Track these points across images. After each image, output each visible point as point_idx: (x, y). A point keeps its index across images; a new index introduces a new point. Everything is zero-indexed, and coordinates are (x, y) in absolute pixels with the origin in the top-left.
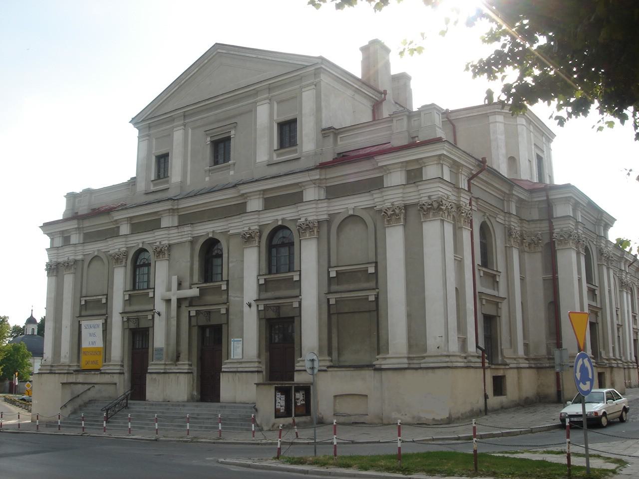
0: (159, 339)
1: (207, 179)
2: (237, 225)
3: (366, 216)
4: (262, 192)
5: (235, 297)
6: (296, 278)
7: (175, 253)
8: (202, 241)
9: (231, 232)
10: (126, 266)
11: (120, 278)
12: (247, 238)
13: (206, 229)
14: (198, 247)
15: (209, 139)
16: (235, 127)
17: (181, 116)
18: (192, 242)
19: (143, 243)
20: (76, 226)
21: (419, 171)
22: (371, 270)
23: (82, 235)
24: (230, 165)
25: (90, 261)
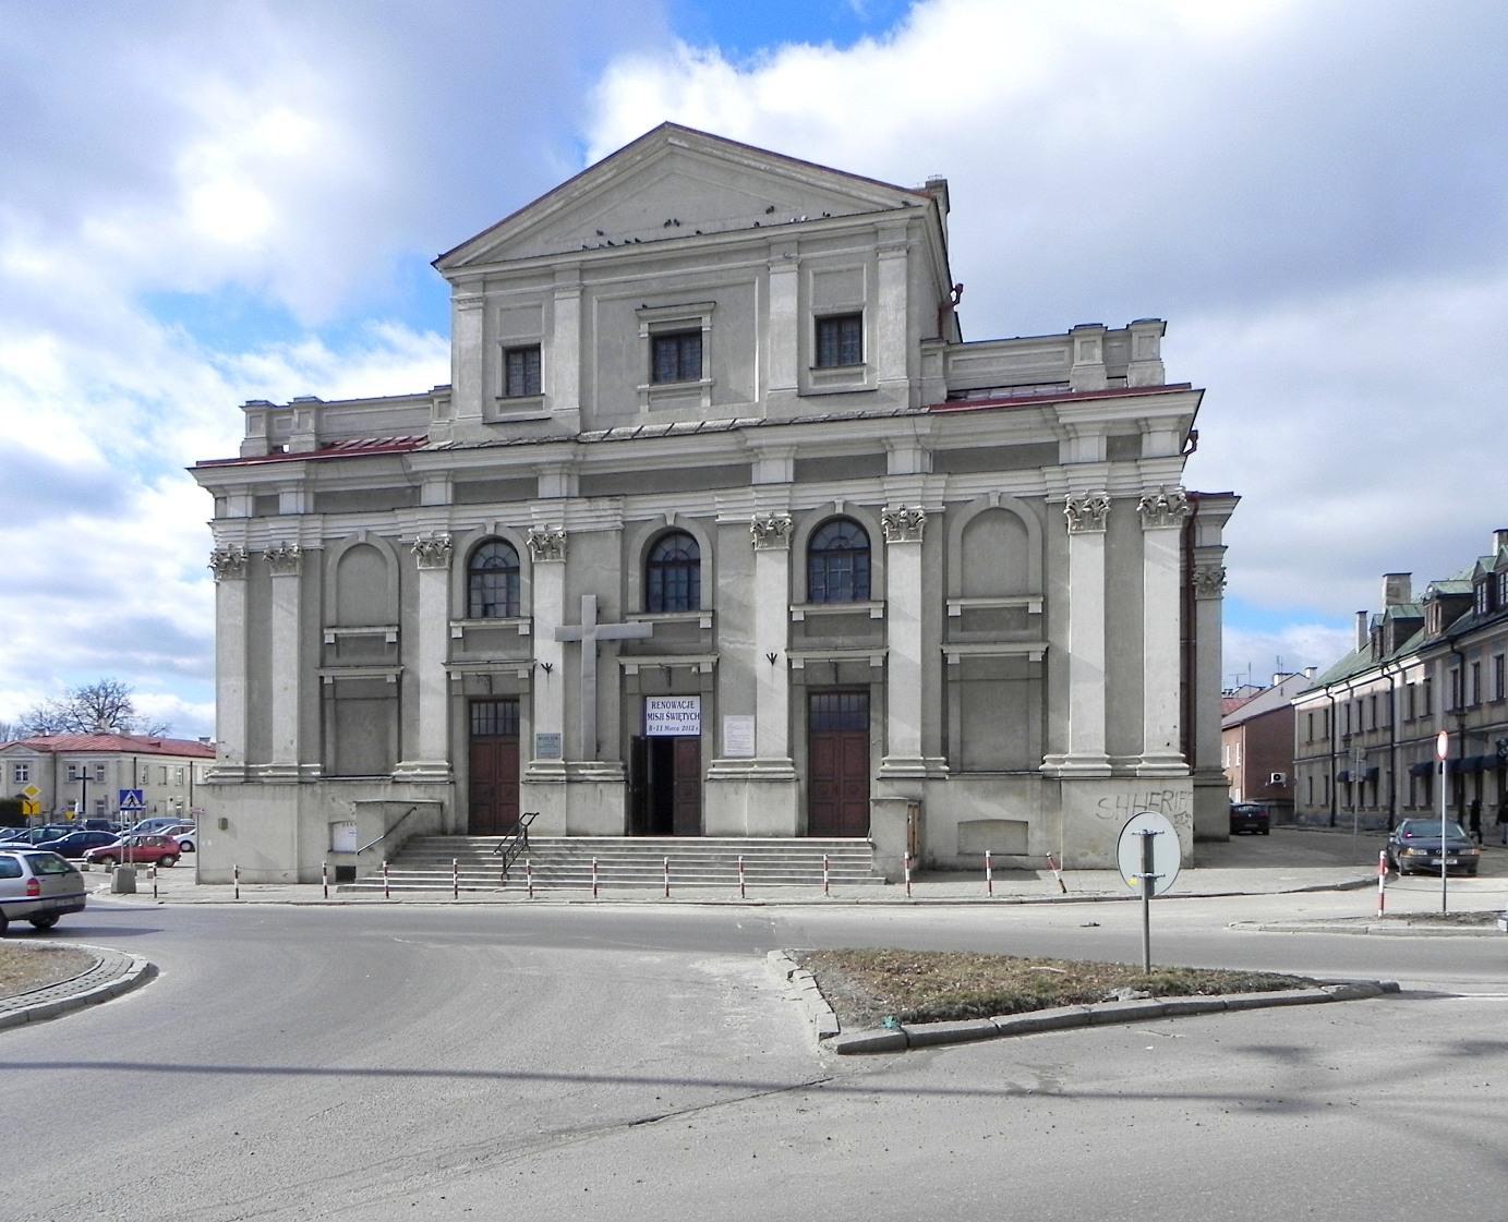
0: (547, 715)
3: (1022, 509)
4: (795, 448)
6: (877, 614)
7: (584, 550)
8: (646, 532)
9: (721, 519)
11: (434, 596)
12: (768, 534)
13: (655, 510)
14: (638, 543)
15: (644, 327)
16: (712, 311)
17: (575, 269)
18: (626, 530)
19: (497, 525)
20: (303, 476)
21: (1136, 441)
22: (1035, 608)
23: (311, 498)
24: (701, 387)
25: (345, 553)
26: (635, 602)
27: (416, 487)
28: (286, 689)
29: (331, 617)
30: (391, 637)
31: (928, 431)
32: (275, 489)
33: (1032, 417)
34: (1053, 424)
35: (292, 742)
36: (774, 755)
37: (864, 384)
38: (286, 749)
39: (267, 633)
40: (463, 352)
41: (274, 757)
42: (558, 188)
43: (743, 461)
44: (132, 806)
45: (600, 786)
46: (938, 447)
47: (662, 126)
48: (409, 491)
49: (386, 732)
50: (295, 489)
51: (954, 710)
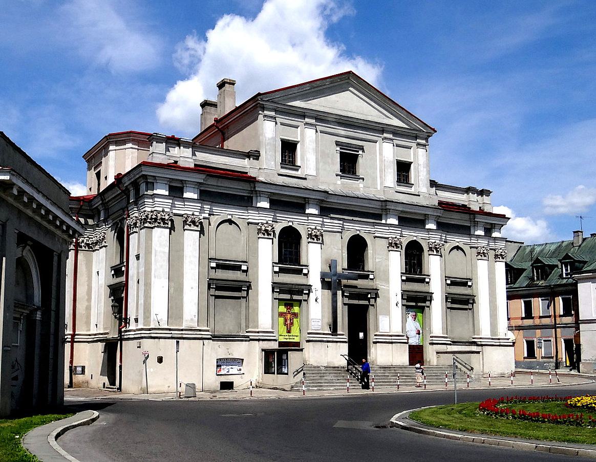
1: (339, 182)
2: (380, 231)
12: (393, 245)
26: (346, 266)
28: (192, 288)
36: (397, 332)
37: (412, 190)
38: (192, 319)
39: (180, 258)
40: (267, 139)
45: (339, 344)
49: (240, 313)
50: (194, 186)
51: (448, 317)
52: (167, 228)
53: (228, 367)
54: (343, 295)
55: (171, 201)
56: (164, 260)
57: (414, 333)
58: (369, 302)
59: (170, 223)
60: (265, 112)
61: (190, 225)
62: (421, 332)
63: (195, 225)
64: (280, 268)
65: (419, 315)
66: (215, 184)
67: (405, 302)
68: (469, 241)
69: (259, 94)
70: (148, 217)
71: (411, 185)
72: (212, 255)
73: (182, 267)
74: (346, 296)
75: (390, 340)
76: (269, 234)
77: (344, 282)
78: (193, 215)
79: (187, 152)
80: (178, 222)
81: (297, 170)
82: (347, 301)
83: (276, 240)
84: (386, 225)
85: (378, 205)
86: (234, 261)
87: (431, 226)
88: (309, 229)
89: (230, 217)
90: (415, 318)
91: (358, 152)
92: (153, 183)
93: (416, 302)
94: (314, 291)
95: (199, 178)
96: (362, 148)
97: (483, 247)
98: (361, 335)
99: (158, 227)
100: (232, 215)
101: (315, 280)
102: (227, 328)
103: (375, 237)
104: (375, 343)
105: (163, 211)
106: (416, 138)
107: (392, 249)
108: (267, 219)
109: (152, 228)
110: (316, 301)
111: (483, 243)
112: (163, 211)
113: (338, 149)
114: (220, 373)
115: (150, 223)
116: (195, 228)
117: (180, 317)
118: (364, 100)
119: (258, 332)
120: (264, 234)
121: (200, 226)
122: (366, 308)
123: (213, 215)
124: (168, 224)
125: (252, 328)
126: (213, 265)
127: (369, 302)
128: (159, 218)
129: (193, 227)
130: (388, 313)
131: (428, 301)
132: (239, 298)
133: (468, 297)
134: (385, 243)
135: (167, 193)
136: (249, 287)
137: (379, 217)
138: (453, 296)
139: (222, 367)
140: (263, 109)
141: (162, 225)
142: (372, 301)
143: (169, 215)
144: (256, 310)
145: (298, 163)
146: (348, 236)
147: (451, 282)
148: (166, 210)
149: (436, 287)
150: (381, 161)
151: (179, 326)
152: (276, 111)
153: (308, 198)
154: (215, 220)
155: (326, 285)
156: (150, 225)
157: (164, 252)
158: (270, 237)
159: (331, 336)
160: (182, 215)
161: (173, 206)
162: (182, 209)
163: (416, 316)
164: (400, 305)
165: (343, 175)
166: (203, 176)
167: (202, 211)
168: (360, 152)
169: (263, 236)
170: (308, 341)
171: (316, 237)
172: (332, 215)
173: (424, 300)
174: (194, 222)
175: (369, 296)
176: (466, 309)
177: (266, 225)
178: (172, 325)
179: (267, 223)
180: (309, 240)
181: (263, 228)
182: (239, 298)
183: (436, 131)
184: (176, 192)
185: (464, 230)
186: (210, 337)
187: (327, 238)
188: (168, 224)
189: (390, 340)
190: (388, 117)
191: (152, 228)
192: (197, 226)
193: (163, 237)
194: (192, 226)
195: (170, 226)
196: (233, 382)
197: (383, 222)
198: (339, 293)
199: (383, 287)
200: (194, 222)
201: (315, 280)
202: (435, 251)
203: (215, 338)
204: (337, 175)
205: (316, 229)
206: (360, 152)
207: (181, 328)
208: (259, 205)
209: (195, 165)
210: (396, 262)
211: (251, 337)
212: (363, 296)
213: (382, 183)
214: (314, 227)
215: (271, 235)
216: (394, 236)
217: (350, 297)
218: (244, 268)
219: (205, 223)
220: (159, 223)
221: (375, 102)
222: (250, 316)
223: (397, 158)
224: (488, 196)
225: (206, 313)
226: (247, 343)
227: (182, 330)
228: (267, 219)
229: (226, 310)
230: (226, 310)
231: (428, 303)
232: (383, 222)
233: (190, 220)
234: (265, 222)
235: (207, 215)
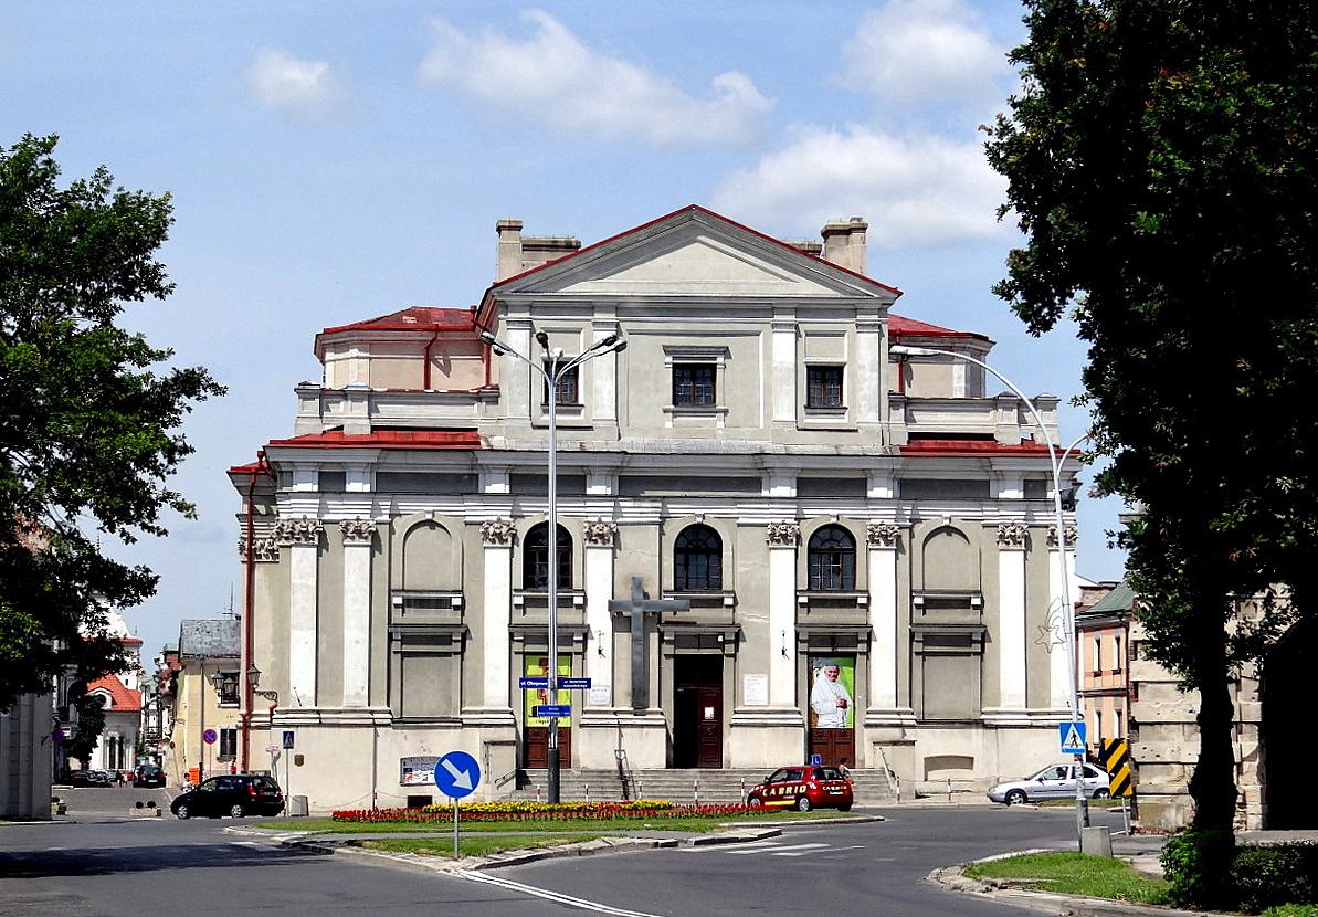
2: (747, 513)
5: (749, 617)
6: (862, 600)
10: (512, 549)
12: (779, 538)
26: (669, 583)
27: (472, 475)
28: (357, 642)
29: (397, 583)
30: (456, 602)
31: (899, 467)
32: (342, 467)
33: (973, 463)
34: (988, 469)
35: (363, 689)
38: (357, 694)
41: (345, 701)
42: (602, 243)
43: (758, 475)
44: (1074, 747)
45: (645, 730)
46: (904, 477)
47: (689, 208)
48: (466, 477)
52: (313, 546)
53: (425, 773)
54: (661, 640)
55: (318, 501)
56: (308, 600)
57: (832, 704)
58: (723, 651)
59: (316, 537)
60: (510, 315)
61: (353, 538)
62: (850, 702)
63: (361, 537)
64: (525, 598)
65: (847, 671)
66: (404, 461)
67: (803, 647)
68: (980, 514)
69: (496, 285)
70: (282, 530)
71: (842, 411)
72: (397, 583)
73: (342, 607)
74: (668, 642)
75: (764, 721)
76: (503, 541)
77: (667, 616)
78: (358, 520)
79: (360, 408)
80: (333, 534)
81: (579, 412)
82: (669, 649)
83: (519, 551)
84: (771, 500)
85: (746, 463)
86: (437, 592)
87: (879, 492)
88: (586, 524)
89: (429, 517)
90: (836, 677)
91: (715, 359)
92: (291, 472)
93: (832, 646)
94: (595, 635)
95: (371, 456)
96: (726, 352)
97: (1013, 524)
98: (709, 712)
99: (296, 545)
100: (433, 512)
101: (598, 618)
102: (425, 705)
103: (739, 525)
104: (732, 726)
105: (305, 519)
106: (855, 311)
107: (775, 545)
108: (500, 513)
109: (290, 547)
110: (600, 652)
111: (1016, 515)
112: (305, 519)
113: (669, 359)
114: (411, 782)
115: (287, 539)
116: (363, 542)
117: (338, 691)
118: (731, 255)
119: (482, 712)
120: (494, 541)
121: (370, 538)
122: (718, 661)
123: (400, 515)
124: (313, 539)
125: (470, 704)
126: (398, 600)
127: (723, 651)
128: (297, 532)
129: (358, 541)
130: (764, 668)
131: (862, 642)
132: (448, 654)
133: (969, 630)
134: (765, 533)
135: (316, 488)
136: (465, 636)
137: (755, 483)
138: (927, 629)
139: (414, 772)
140: (506, 308)
141: (303, 541)
142: (729, 649)
143: (315, 524)
144: (480, 673)
145: (581, 401)
146: (674, 529)
147: (925, 600)
148: (309, 516)
149: (884, 614)
150: (768, 369)
151: (337, 705)
152: (531, 308)
153: (587, 466)
154: (401, 525)
155: (620, 620)
156: (287, 543)
157: (308, 586)
158: (505, 545)
159: (632, 716)
160: (336, 522)
161: (322, 509)
162: (340, 511)
163: (837, 671)
164: (791, 652)
165: (677, 409)
166: (377, 452)
167: (375, 511)
168: (720, 360)
169: (491, 545)
170: (582, 726)
171: (609, 538)
172: (647, 493)
173: (855, 640)
174: (358, 532)
175: (720, 639)
176: (968, 654)
177: (496, 525)
178: (324, 703)
179: (499, 521)
180: (587, 544)
181: (491, 530)
182: (448, 654)
183: (900, 294)
184: (332, 482)
185: (976, 491)
186: (389, 721)
187: (626, 537)
188: (313, 539)
189: (764, 721)
190: (787, 279)
191: (290, 547)
192: (366, 538)
193: (305, 561)
194: (357, 538)
195: (316, 542)
196: (431, 797)
197: (765, 493)
198: (654, 637)
199: (756, 620)
200: (358, 532)
201: (598, 618)
202: (882, 542)
203: (399, 722)
204: (665, 412)
205: (600, 522)
206: (720, 360)
207: (341, 708)
208: (489, 490)
209: (374, 428)
210: (783, 573)
211: (464, 722)
212: (711, 640)
213: (768, 415)
214: (596, 519)
215: (507, 541)
216: (780, 521)
217: (676, 642)
218: (456, 602)
219: (384, 532)
220: (299, 539)
221: (756, 255)
222: (466, 688)
223: (808, 359)
224: (1051, 410)
225: (389, 682)
226: (459, 731)
227: (340, 712)
228: (500, 513)
229: (424, 674)
230: (424, 674)
231: (862, 647)
232: (765, 493)
233: (351, 528)
234: (495, 519)
235: (386, 518)
